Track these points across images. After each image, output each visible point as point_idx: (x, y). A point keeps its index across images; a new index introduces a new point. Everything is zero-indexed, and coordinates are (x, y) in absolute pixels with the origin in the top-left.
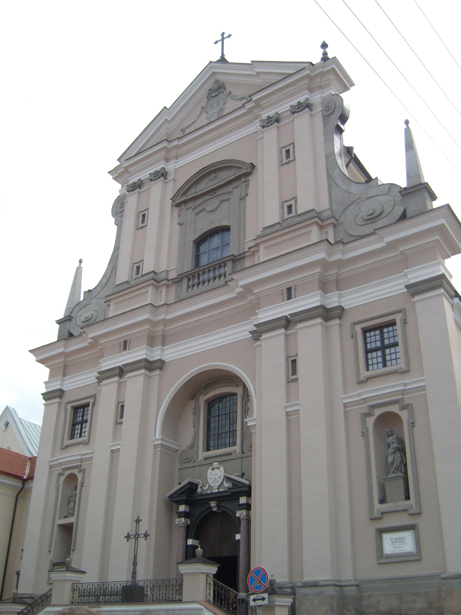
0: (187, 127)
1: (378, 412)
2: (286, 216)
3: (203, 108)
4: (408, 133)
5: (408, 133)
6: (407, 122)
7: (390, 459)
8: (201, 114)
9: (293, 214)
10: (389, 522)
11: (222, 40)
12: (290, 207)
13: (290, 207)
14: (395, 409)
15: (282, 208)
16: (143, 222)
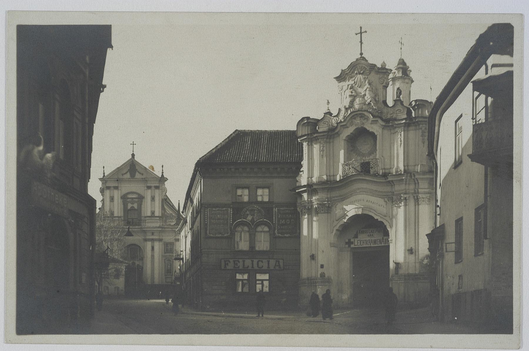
0: (125, 174)
1: (168, 259)
2: (152, 215)
3: (128, 170)
4: (179, 203)
5: (179, 203)
6: (179, 201)
7: (169, 267)
8: (128, 171)
9: (154, 215)
10: (168, 276)
11: (133, 144)
12: (153, 213)
13: (153, 213)
14: (170, 259)
15: (151, 212)
16: (112, 200)
